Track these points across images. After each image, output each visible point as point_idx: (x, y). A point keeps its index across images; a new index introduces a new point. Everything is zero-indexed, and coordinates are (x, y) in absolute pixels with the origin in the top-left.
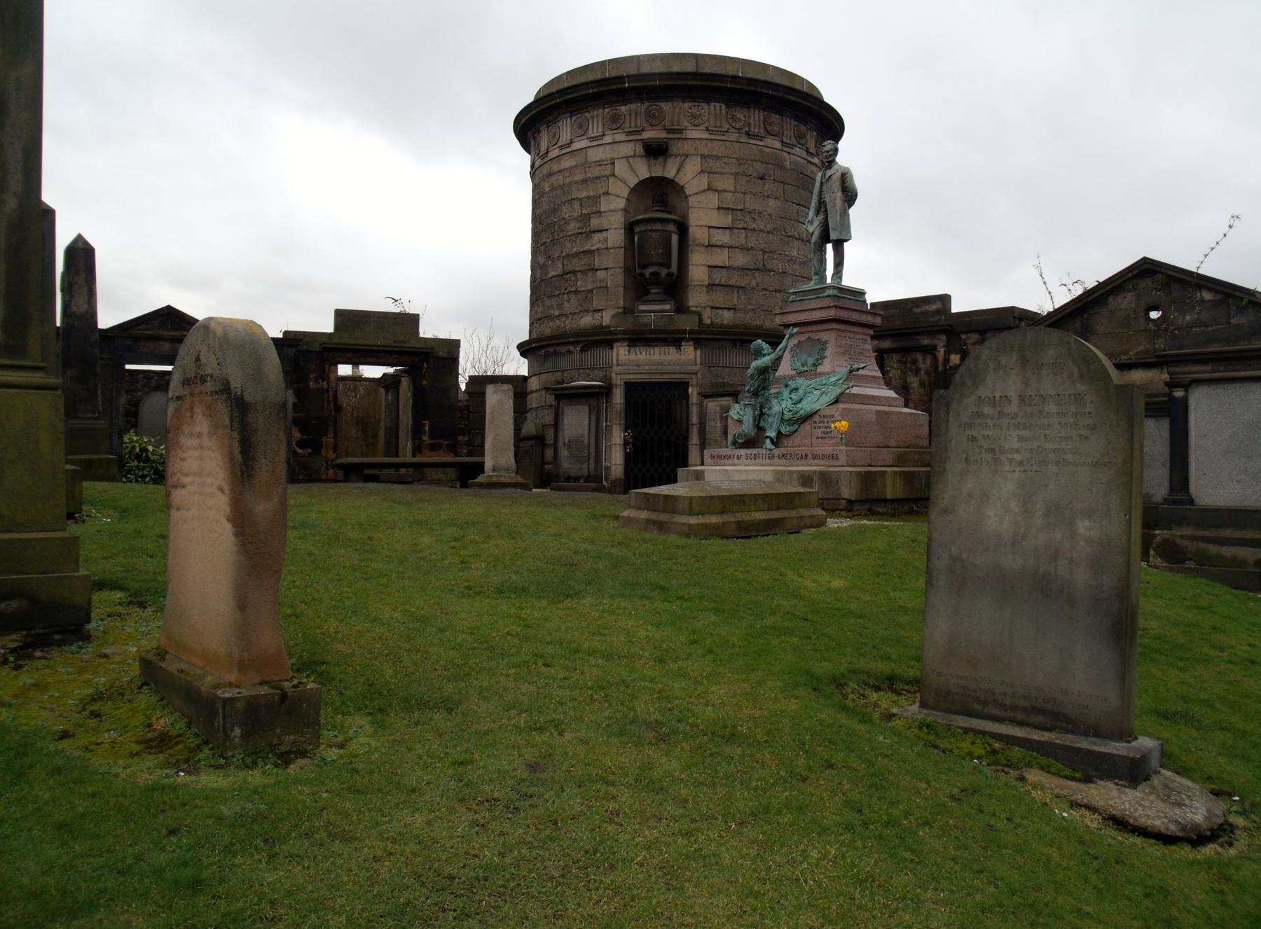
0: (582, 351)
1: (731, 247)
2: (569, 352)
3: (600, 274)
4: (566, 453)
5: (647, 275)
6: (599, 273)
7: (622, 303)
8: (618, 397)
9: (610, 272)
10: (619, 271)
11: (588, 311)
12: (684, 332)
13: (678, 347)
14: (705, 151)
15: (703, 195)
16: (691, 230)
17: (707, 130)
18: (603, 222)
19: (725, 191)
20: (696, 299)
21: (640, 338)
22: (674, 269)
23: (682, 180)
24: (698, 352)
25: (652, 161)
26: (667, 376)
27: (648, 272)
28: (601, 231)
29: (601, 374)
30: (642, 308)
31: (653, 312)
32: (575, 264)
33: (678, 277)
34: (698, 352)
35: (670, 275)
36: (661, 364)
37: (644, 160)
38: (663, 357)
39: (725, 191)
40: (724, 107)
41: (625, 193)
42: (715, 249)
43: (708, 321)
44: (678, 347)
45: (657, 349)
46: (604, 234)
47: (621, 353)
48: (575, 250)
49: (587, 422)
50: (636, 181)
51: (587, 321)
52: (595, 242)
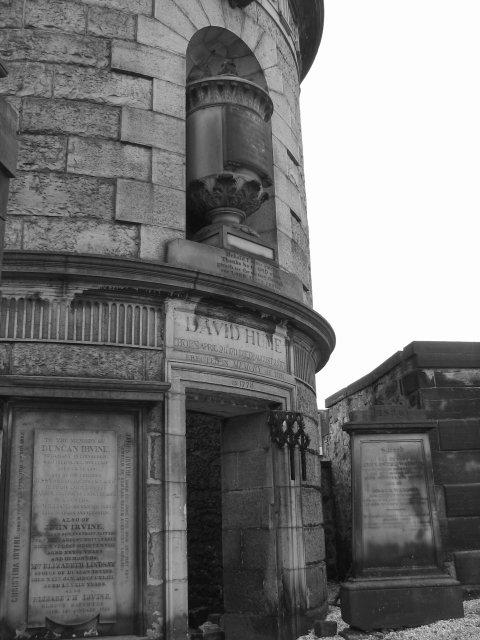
0: (78, 303)
2: (40, 302)
4: (39, 557)
5: (240, 184)
6: (129, 149)
8: (176, 424)
11: (99, 220)
13: (270, 332)
26: (257, 387)
27: (243, 177)
28: (136, 75)
30: (233, 241)
32: (64, 118)
36: (248, 360)
41: (190, 34)
44: (270, 332)
45: (242, 329)
47: (179, 319)
48: (60, 91)
49: (109, 473)
51: (95, 239)
52: (122, 90)
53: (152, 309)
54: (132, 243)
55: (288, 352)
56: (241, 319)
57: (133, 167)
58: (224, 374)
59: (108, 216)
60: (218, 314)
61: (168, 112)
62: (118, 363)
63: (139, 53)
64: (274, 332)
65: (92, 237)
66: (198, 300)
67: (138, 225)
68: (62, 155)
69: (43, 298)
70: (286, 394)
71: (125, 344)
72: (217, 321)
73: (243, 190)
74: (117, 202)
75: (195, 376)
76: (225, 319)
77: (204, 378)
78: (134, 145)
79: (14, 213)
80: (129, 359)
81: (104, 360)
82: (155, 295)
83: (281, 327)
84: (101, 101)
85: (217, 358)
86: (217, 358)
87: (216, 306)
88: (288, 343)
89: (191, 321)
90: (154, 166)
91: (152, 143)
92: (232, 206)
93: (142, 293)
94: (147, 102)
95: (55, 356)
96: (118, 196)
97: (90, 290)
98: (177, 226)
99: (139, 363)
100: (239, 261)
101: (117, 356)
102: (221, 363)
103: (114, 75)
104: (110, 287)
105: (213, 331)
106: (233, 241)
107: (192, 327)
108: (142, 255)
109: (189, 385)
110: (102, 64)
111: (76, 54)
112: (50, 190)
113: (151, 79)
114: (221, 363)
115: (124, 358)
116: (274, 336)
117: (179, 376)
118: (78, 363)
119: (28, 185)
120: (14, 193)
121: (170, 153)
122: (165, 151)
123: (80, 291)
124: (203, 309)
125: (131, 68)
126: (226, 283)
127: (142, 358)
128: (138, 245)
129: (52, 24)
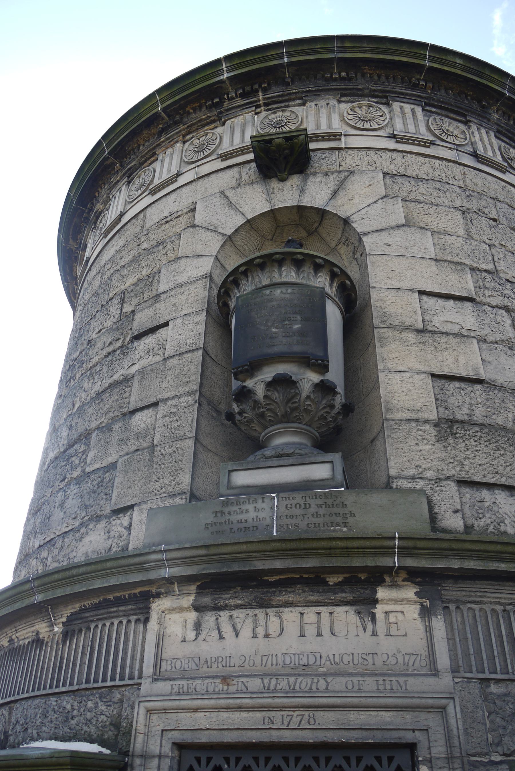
1: (482, 340)
2: (38, 642)
3: (140, 420)
5: (260, 391)
7: (186, 479)
9: (162, 409)
10: (190, 400)
11: (98, 518)
12: (380, 544)
13: (366, 604)
14: (393, 169)
15: (395, 232)
16: (374, 296)
17: (393, 136)
18: (162, 311)
19: (446, 233)
20: (409, 455)
21: (235, 577)
22: (335, 374)
23: (341, 207)
24: (439, 623)
25: (275, 184)
26: (327, 718)
29: (105, 711)
30: (243, 478)
31: (280, 486)
33: (348, 409)
34: (439, 623)
35: (325, 388)
36: (305, 670)
37: (259, 188)
38: (312, 645)
39: (446, 233)
40: (419, 110)
42: (443, 339)
43: (455, 523)
44: (366, 604)
45: (291, 615)
46: (162, 333)
47: (174, 625)
50: (240, 221)
53: (137, 621)
54: (125, 532)
55: (429, 631)
56: (284, 597)
57: (139, 436)
58: (240, 708)
59: (107, 511)
60: (232, 602)
61: (183, 350)
62: (89, 715)
63: (157, 305)
64: (375, 602)
65: (91, 542)
66: (193, 588)
67: (131, 507)
68: (84, 456)
69: (41, 636)
70: (432, 720)
71: (100, 684)
72: (236, 613)
73: (265, 397)
74: (115, 488)
75: (187, 720)
76: (249, 606)
77: (202, 720)
78: (142, 409)
79: (48, 539)
80: (102, 707)
81: (75, 712)
82: (134, 599)
83: (394, 585)
84: (122, 377)
85: (225, 679)
86: (225, 679)
87: (228, 589)
88: (426, 613)
89: (190, 625)
90: (159, 423)
91: (159, 397)
92: (272, 423)
93: (119, 601)
94: (161, 352)
95: (36, 716)
96: (117, 480)
97: (72, 614)
98: (179, 488)
99: (113, 710)
100: (244, 507)
101: (90, 704)
102: (233, 689)
103: (136, 344)
104: (86, 603)
105: (227, 630)
106: (243, 478)
107: (191, 635)
108: (131, 548)
109: (177, 737)
110: (128, 339)
111: (111, 343)
112: (69, 503)
113: (166, 324)
114: (233, 689)
115: (96, 707)
116: (379, 610)
117: (158, 723)
118: (51, 722)
119: (57, 504)
120: (49, 518)
121: (179, 397)
122: (173, 398)
123: (64, 619)
124: (206, 600)
125: (150, 325)
126: (213, 551)
127: (121, 701)
128: (130, 534)
129: (101, 327)
